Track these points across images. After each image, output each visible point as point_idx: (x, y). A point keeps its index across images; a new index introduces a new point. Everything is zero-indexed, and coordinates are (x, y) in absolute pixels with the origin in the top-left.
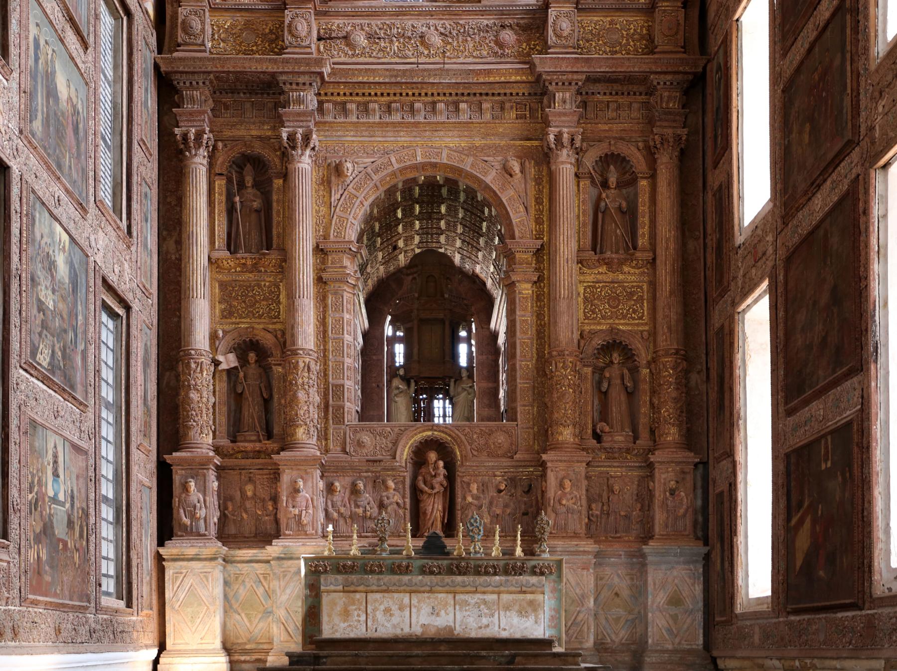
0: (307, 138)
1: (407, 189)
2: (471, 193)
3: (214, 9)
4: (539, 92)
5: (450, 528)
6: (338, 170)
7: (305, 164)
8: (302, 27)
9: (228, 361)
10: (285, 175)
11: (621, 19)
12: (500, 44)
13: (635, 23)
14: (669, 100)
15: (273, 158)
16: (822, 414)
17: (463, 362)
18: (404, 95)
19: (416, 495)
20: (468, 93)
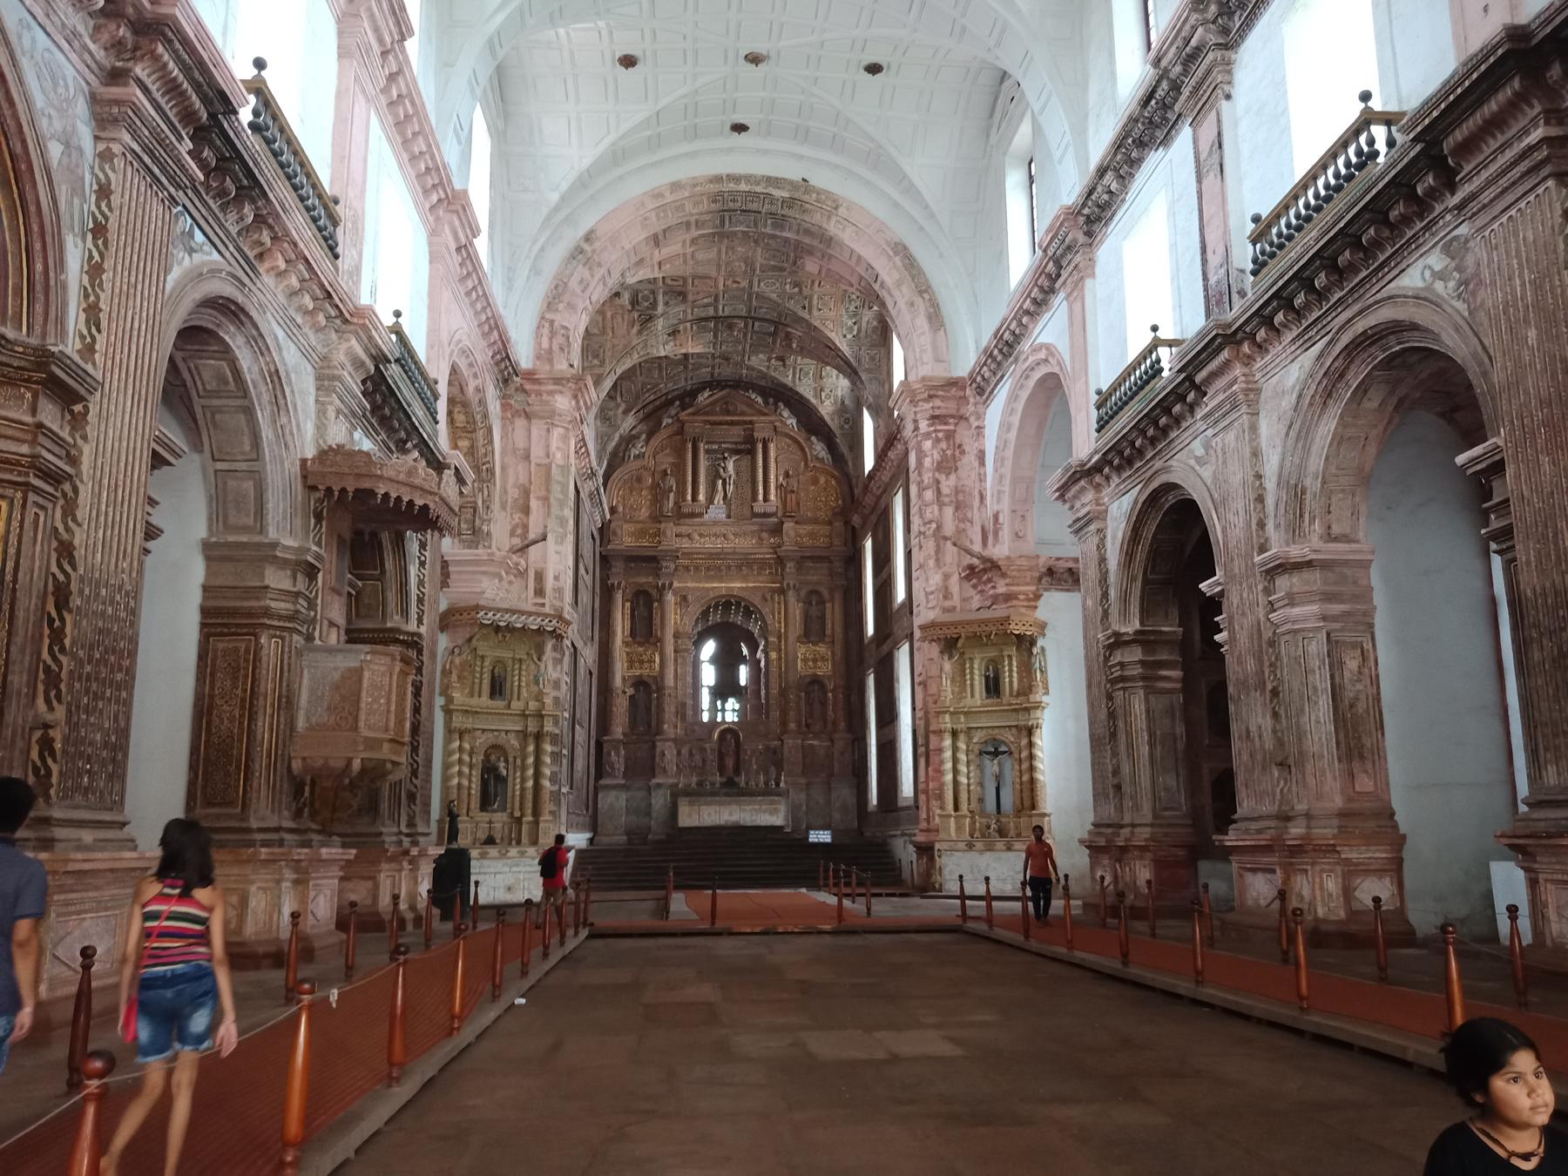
0: (671, 584)
1: (716, 606)
2: (746, 608)
3: (627, 522)
4: (780, 561)
5: (737, 771)
6: (684, 598)
7: (670, 597)
8: (669, 533)
9: (630, 691)
10: (661, 600)
11: (817, 527)
12: (761, 539)
13: (825, 529)
14: (838, 566)
15: (654, 593)
16: (886, 730)
17: (743, 682)
18: (716, 564)
19: (720, 753)
20: (745, 563)
